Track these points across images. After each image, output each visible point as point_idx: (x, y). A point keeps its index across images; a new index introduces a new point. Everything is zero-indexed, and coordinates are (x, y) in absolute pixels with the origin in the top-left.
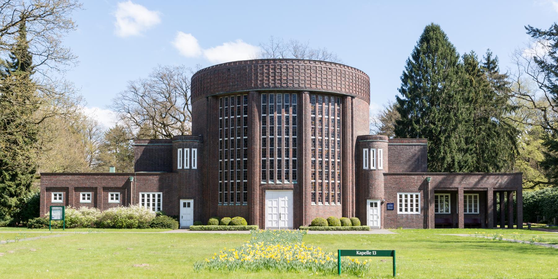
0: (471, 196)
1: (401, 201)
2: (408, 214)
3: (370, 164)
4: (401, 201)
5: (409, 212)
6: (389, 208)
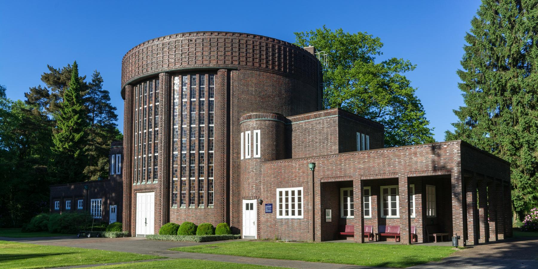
0: (387, 189)
1: (281, 200)
2: (288, 219)
3: (252, 151)
4: (281, 200)
5: (290, 216)
6: (267, 211)
